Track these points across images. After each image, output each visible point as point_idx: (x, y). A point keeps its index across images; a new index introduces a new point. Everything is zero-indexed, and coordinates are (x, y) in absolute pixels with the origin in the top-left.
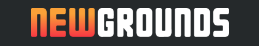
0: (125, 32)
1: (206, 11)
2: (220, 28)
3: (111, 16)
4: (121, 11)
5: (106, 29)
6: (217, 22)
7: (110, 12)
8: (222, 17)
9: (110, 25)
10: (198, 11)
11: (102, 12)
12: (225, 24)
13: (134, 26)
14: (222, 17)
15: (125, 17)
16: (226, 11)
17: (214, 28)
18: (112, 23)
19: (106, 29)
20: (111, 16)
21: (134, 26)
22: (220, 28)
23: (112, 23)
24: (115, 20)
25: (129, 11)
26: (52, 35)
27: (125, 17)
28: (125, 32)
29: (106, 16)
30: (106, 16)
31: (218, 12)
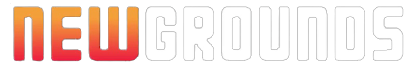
0: (198, 52)
1: (358, 13)
2: (386, 44)
3: (171, 19)
4: (190, 13)
5: (161, 45)
6: (381, 32)
7: (169, 15)
8: (390, 22)
9: (169, 38)
10: (342, 13)
11: (153, 13)
12: (396, 36)
13: (216, 41)
14: (390, 22)
15: (199, 22)
16: (397, 12)
17: (373, 44)
18: (173, 35)
19: (161, 45)
20: (171, 19)
21: (216, 41)
22: (386, 44)
23: (173, 35)
24: (179, 29)
25: (207, 13)
26: (338, 57)
27: (199, 22)
28: (198, 52)
29: (160, 21)
30: (160, 21)
31: (381, 13)
